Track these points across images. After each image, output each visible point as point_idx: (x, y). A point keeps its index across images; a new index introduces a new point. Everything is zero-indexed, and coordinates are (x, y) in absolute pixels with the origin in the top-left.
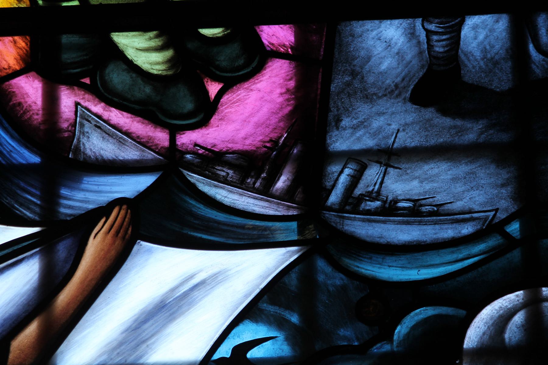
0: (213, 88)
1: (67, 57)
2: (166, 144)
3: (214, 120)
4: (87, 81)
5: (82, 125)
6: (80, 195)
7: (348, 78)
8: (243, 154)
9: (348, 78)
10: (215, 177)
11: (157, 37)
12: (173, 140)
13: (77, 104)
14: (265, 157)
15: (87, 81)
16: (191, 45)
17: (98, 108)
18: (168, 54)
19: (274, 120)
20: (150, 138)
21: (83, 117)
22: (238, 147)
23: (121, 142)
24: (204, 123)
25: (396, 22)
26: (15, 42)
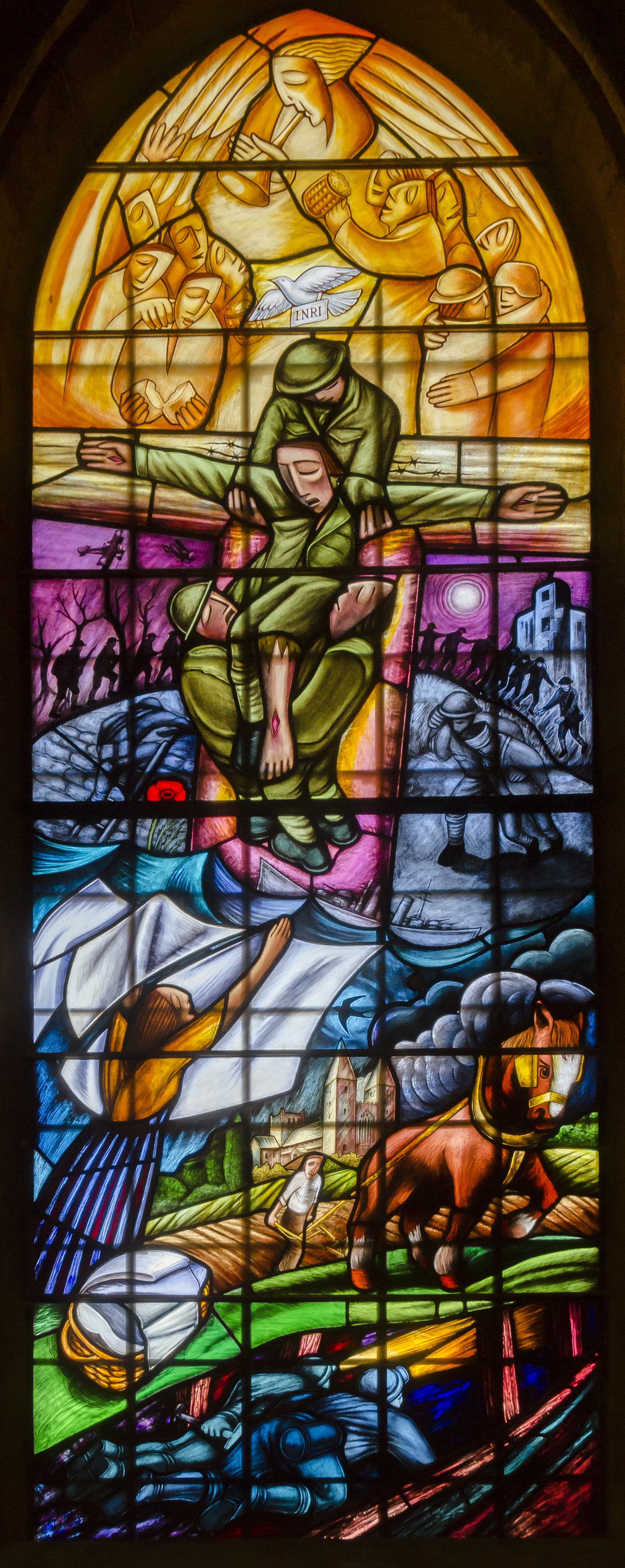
0: (333, 851)
1: (255, 830)
2: (308, 883)
3: (333, 870)
4: (266, 845)
5: (264, 871)
6: (263, 912)
7: (405, 848)
8: (350, 891)
9: (405, 848)
10: (334, 904)
11: (304, 819)
12: (312, 881)
13: (261, 858)
14: (362, 892)
15: (266, 845)
16: (322, 825)
17: (272, 861)
18: (310, 829)
19: (366, 872)
20: (300, 880)
21: (264, 866)
22: (346, 887)
23: (284, 881)
24: (328, 872)
25: (431, 815)
26: (228, 821)
